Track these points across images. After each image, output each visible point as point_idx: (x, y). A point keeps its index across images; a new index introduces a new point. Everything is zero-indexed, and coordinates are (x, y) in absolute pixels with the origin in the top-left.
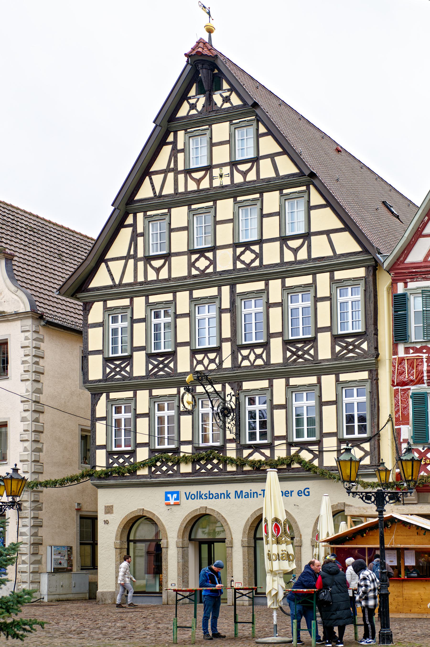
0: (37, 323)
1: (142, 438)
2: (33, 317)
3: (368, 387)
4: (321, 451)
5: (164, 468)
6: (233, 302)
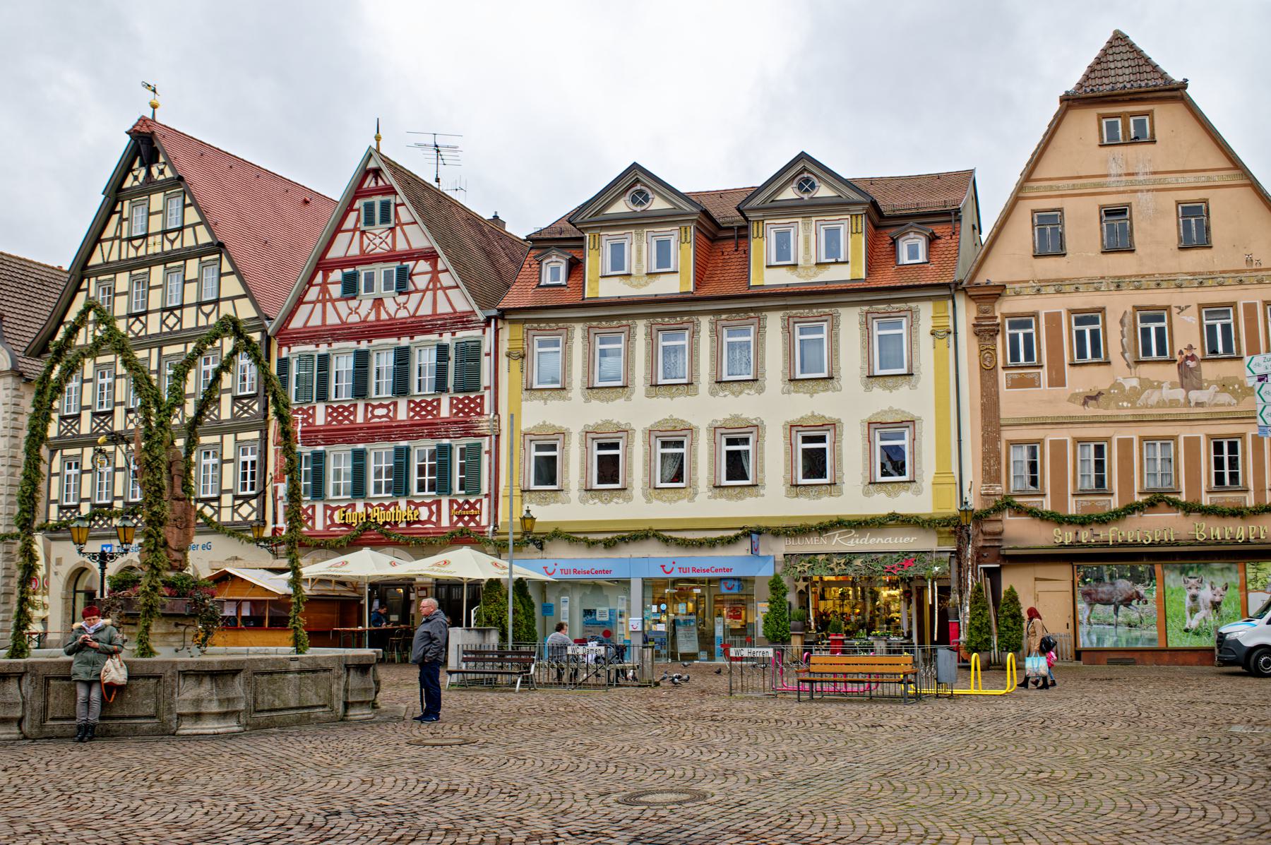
0: (17, 380)
1: (86, 493)
2: (13, 375)
3: (258, 446)
4: (220, 507)
5: (101, 522)
6: (159, 365)
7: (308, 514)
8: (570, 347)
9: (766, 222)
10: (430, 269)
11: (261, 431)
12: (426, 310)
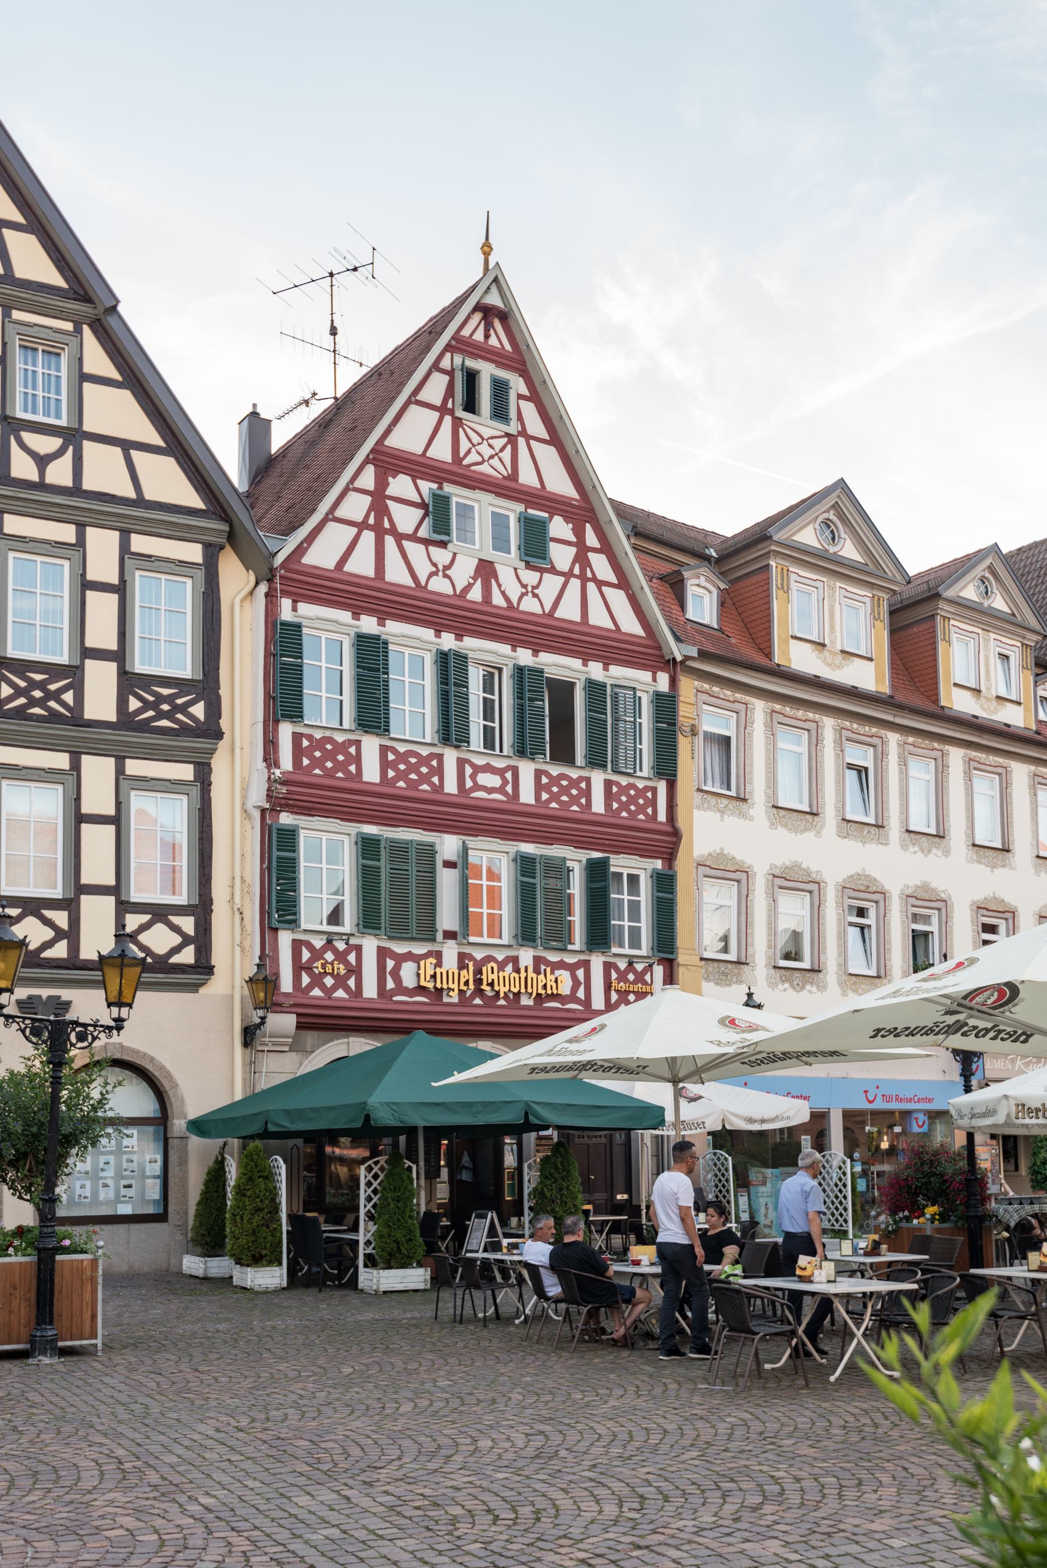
7: (347, 963)
8: (751, 735)
9: (952, 622)
10: (574, 539)
11: (196, 764)
12: (569, 611)
